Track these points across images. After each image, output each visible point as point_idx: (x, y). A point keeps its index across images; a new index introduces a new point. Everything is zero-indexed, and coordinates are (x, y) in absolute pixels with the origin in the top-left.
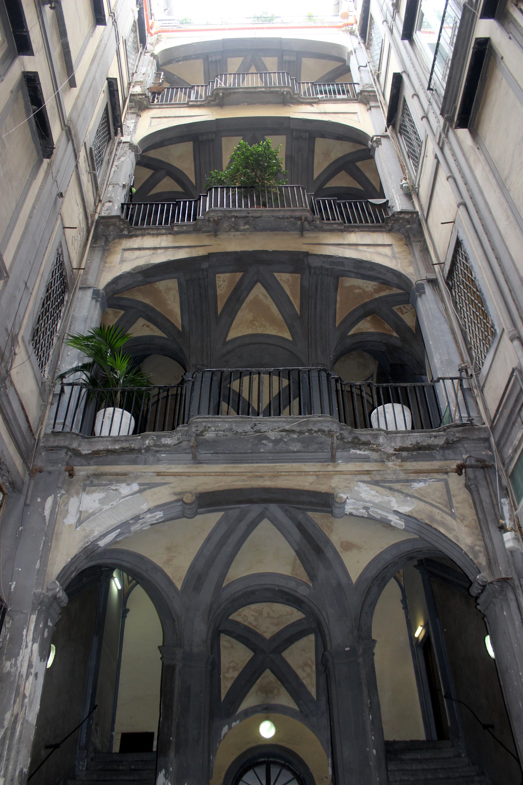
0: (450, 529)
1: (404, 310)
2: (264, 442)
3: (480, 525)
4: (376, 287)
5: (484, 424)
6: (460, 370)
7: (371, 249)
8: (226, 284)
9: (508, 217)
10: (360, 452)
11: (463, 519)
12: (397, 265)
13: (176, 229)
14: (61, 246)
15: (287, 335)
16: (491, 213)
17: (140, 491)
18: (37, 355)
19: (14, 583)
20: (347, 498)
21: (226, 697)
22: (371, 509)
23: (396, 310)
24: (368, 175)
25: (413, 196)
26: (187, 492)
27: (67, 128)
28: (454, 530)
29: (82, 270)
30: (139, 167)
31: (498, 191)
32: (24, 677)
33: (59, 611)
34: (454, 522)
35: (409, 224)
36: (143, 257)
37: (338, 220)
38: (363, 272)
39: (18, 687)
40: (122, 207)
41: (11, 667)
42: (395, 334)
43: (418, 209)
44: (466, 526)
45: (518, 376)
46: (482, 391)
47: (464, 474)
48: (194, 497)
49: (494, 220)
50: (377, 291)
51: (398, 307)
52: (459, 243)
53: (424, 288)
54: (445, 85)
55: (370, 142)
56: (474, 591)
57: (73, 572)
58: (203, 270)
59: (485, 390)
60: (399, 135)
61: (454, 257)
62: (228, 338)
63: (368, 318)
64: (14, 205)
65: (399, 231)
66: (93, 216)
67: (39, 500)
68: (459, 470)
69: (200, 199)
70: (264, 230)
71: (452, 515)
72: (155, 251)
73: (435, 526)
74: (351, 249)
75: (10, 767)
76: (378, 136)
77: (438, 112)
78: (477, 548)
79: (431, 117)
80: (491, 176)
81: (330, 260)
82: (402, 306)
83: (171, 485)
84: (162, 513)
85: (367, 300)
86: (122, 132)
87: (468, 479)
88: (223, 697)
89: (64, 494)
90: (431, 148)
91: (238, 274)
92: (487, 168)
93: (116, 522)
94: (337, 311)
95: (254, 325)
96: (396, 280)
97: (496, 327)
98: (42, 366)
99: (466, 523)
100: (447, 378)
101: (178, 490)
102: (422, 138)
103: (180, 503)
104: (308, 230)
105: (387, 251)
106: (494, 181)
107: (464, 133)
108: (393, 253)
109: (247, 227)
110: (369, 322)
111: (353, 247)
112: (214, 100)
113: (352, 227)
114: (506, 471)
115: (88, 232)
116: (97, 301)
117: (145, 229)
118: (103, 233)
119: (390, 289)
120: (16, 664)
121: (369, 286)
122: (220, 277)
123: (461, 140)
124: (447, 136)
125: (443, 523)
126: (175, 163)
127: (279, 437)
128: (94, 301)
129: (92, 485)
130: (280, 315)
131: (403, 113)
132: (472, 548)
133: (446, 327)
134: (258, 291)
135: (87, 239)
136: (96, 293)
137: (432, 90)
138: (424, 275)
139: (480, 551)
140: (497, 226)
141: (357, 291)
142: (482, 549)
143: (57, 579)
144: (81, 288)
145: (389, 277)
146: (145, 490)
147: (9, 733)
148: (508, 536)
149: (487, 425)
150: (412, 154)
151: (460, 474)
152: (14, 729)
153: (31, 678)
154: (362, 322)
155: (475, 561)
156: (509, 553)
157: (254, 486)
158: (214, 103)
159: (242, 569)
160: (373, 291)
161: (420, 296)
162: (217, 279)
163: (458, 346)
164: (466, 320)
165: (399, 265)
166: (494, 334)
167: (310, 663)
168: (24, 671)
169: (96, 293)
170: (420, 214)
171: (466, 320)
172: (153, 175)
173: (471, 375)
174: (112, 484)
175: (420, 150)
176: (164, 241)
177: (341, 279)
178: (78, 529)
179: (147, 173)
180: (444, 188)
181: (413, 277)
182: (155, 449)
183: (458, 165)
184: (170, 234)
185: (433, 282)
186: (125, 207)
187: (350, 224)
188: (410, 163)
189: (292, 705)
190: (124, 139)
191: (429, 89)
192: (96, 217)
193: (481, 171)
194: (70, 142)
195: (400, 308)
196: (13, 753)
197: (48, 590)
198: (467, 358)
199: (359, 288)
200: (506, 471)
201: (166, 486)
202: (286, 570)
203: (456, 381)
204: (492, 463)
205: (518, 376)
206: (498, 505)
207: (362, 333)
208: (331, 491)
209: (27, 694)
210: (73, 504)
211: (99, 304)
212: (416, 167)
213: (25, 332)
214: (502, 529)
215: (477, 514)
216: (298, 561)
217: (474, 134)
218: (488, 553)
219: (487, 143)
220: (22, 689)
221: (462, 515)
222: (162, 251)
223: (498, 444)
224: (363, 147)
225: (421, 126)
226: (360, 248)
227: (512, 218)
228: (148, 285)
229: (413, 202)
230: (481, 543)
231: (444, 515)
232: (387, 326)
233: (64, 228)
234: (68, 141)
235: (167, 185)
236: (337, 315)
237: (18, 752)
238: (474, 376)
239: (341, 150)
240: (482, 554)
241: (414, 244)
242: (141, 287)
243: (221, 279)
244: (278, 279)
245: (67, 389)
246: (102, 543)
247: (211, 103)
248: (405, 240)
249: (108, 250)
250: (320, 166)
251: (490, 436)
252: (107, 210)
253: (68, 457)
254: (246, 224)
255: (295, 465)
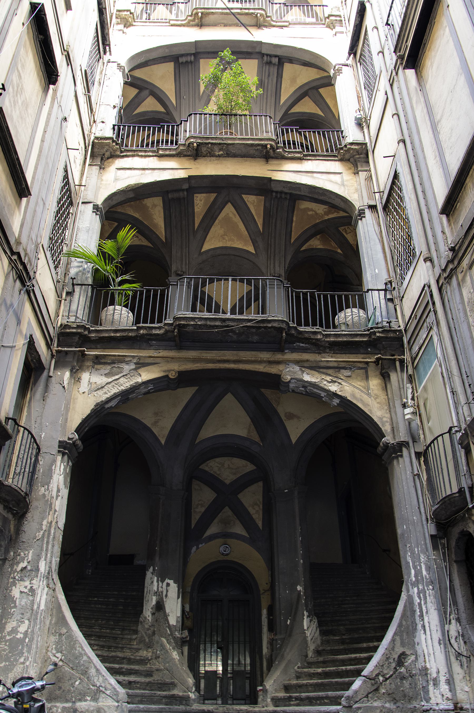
0: (367, 405)
1: (348, 231)
2: (230, 334)
3: (389, 403)
4: (326, 210)
5: (399, 327)
6: (386, 284)
7: (324, 176)
8: (202, 202)
9: (436, 157)
10: (303, 345)
11: (376, 398)
12: (345, 192)
13: (161, 152)
14: (66, 166)
15: (251, 249)
16: (423, 151)
17: (136, 369)
18: (52, 260)
19: (44, 433)
20: (291, 379)
21: (195, 526)
22: (308, 388)
23: (341, 230)
24: (328, 101)
25: (365, 127)
26: (171, 370)
27: (66, 53)
28: (368, 405)
29: (83, 187)
30: (126, 86)
31: (431, 132)
32: (55, 498)
33: (76, 455)
34: (370, 400)
35: (359, 154)
36: (133, 176)
37: (299, 148)
38: (316, 196)
39: (51, 504)
40: (114, 129)
41: (45, 491)
42: (339, 251)
43: (367, 141)
44: (378, 403)
45: (427, 290)
46: (401, 300)
47: (380, 365)
48: (177, 374)
49: (425, 158)
50: (327, 213)
51: (343, 228)
52: (396, 176)
53: (364, 213)
54: (400, 23)
55: (332, 70)
56: (380, 449)
57: (86, 427)
58: (183, 190)
59: (404, 300)
60: (358, 64)
61: (391, 189)
62: (203, 250)
63: (318, 237)
64: (30, 131)
65: (349, 160)
66: (89, 136)
67: (59, 374)
68: (377, 362)
69: (181, 124)
70: (235, 156)
71: (369, 394)
72: (143, 172)
73: (355, 402)
74: (307, 176)
75: (49, 555)
76: (340, 65)
77: (393, 50)
78: (385, 419)
79: (386, 52)
80: (427, 118)
81: (289, 185)
82: (346, 227)
83: (160, 365)
84: (152, 385)
85: (317, 221)
86: (110, 51)
87: (382, 368)
88: (193, 526)
89: (78, 370)
90: (383, 84)
91: (212, 194)
92: (425, 110)
93: (118, 391)
94: (293, 229)
95: (224, 239)
96: (342, 205)
97: (416, 250)
98: (56, 267)
99: (378, 400)
100: (375, 290)
101: (165, 368)
102: (377, 72)
103: (166, 379)
104: (272, 158)
105: (337, 178)
106: (429, 123)
107: (411, 73)
108: (343, 181)
109: (221, 153)
110: (319, 240)
111: (309, 174)
112: (194, 20)
113: (310, 155)
114: (413, 364)
115: (86, 152)
116: (96, 214)
117: (134, 151)
118: (101, 153)
119: (338, 213)
120: (48, 489)
121: (320, 209)
122: (197, 197)
123: (408, 80)
124: (397, 74)
125: (361, 400)
126: (158, 83)
127: (242, 331)
128: (95, 214)
129: (100, 363)
130: (246, 231)
131: (364, 42)
132: (381, 419)
133: (379, 247)
134: (229, 210)
135: (86, 158)
136: (96, 208)
137: (389, 25)
138: (367, 201)
139: (387, 422)
140: (426, 164)
141: (310, 213)
142: (389, 420)
143: (75, 431)
144: (83, 203)
145: (337, 202)
146: (139, 368)
147: (46, 533)
148: (407, 411)
149: (402, 328)
150: (368, 86)
151: (377, 365)
152: (49, 531)
153: (59, 498)
154: (313, 239)
155: (383, 429)
156: (407, 423)
157: (222, 368)
158: (193, 23)
159: (210, 430)
160: (323, 214)
161: (361, 219)
162: (195, 198)
163: (387, 263)
164: (396, 242)
165: (346, 192)
166: (414, 255)
167: (258, 503)
168: (54, 494)
169: (96, 208)
170: (368, 145)
171: (396, 242)
172: (138, 94)
173: (394, 288)
174: (115, 363)
175: (375, 83)
176: (153, 162)
177: (297, 202)
178: (90, 395)
179: (133, 92)
180: (390, 125)
181: (356, 203)
182: (148, 337)
183: (403, 104)
184: (156, 156)
185: (373, 208)
186: (116, 127)
187: (309, 152)
188: (365, 93)
189: (244, 533)
190: (112, 58)
191: (387, 24)
192: (92, 138)
193: (420, 112)
194: (70, 66)
195: (345, 229)
196: (50, 546)
197: (69, 439)
198: (392, 274)
199: (312, 210)
200: (413, 364)
201: (156, 365)
202: (243, 433)
203: (382, 293)
204: (403, 357)
205: (427, 290)
206: (404, 388)
207: (312, 249)
208: (280, 373)
209: (57, 510)
210: (85, 376)
211: (98, 216)
212: (370, 99)
213: (45, 242)
214: (404, 406)
215: (387, 395)
216: (253, 427)
217: (419, 76)
218: (392, 423)
219: (428, 86)
220: (53, 506)
221: (376, 395)
222: (150, 171)
223: (409, 342)
224: (326, 74)
225: (377, 61)
226: (315, 175)
227: (438, 158)
228: (138, 202)
229: (363, 132)
230: (388, 415)
231: (363, 394)
232: (333, 244)
233: (68, 149)
234: (68, 65)
235: (150, 105)
236: (293, 233)
237: (53, 546)
238: (396, 289)
239: (306, 76)
240: (388, 423)
241: (360, 173)
242: (132, 203)
243: (198, 199)
244: (246, 200)
245: (77, 289)
246: (107, 406)
247: (191, 23)
248: (353, 168)
249: (104, 169)
250: (287, 92)
251: (403, 336)
252: (101, 130)
253: (81, 341)
254: (220, 150)
255: (253, 353)
